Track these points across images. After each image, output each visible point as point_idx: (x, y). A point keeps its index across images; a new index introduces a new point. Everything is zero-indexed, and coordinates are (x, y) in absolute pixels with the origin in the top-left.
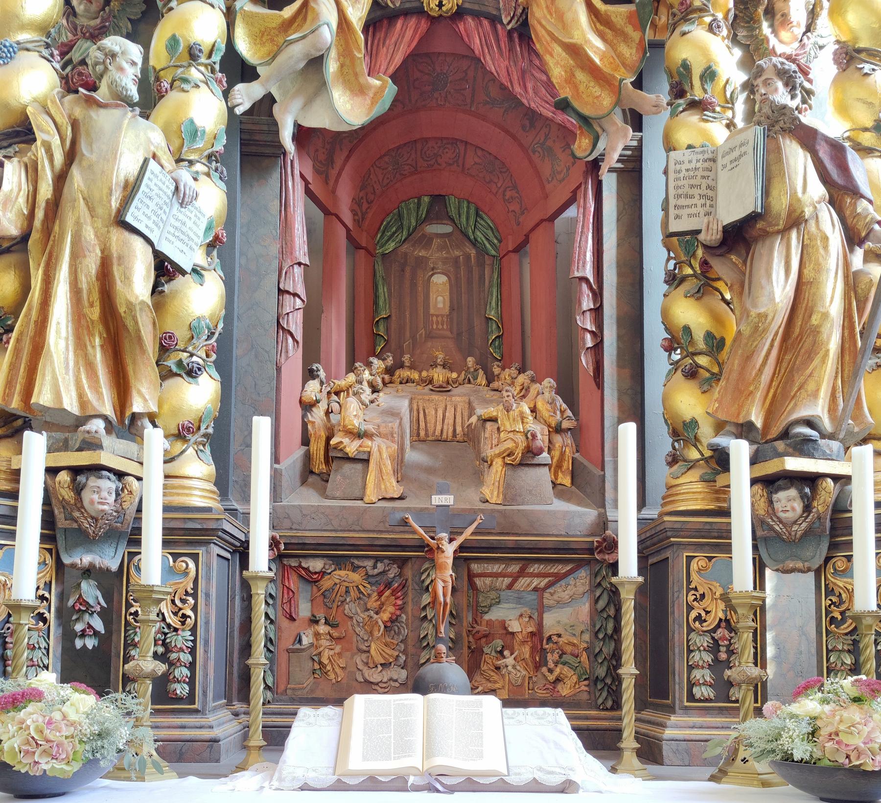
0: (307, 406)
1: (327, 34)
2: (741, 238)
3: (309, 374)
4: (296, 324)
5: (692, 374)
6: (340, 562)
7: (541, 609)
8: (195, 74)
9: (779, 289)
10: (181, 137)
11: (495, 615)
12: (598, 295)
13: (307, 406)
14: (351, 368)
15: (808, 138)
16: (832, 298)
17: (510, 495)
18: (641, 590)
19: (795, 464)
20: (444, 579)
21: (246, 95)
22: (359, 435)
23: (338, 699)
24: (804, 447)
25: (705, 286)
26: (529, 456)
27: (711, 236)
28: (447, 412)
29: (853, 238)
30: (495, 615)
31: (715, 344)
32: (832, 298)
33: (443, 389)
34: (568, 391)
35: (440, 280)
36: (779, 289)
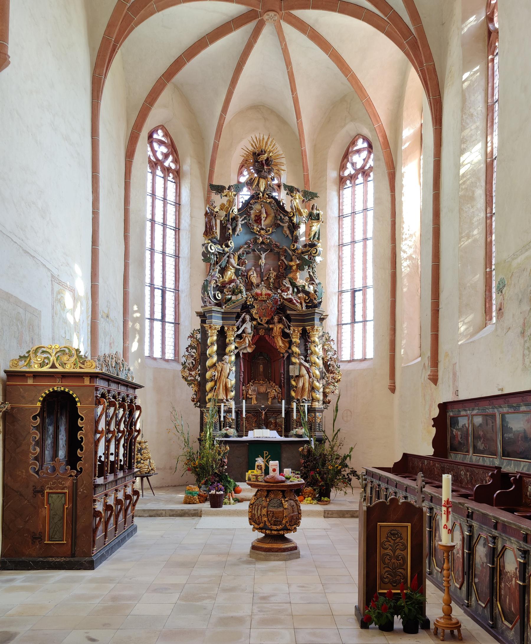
0: (243, 390)
1: (247, 345)
2: (297, 376)
3: (243, 385)
4: (242, 380)
5: (294, 390)
6: (248, 413)
7: (276, 419)
8: (232, 353)
9: (301, 384)
10: (231, 362)
11: (270, 420)
12: (284, 375)
13: (243, 390)
14: (248, 383)
15: (305, 367)
16: (307, 385)
17: (272, 403)
18: (285, 418)
19: (302, 404)
20: (263, 417)
21: (236, 351)
22: (251, 395)
23: (253, 430)
24: (303, 402)
25: (294, 381)
26: (274, 398)
27: (294, 376)
28: (262, 389)
29: (310, 377)
30: (270, 420)
31: (296, 387)
32: (307, 385)
33: (262, 385)
34: (280, 387)
35: (261, 366)
36: (301, 384)
